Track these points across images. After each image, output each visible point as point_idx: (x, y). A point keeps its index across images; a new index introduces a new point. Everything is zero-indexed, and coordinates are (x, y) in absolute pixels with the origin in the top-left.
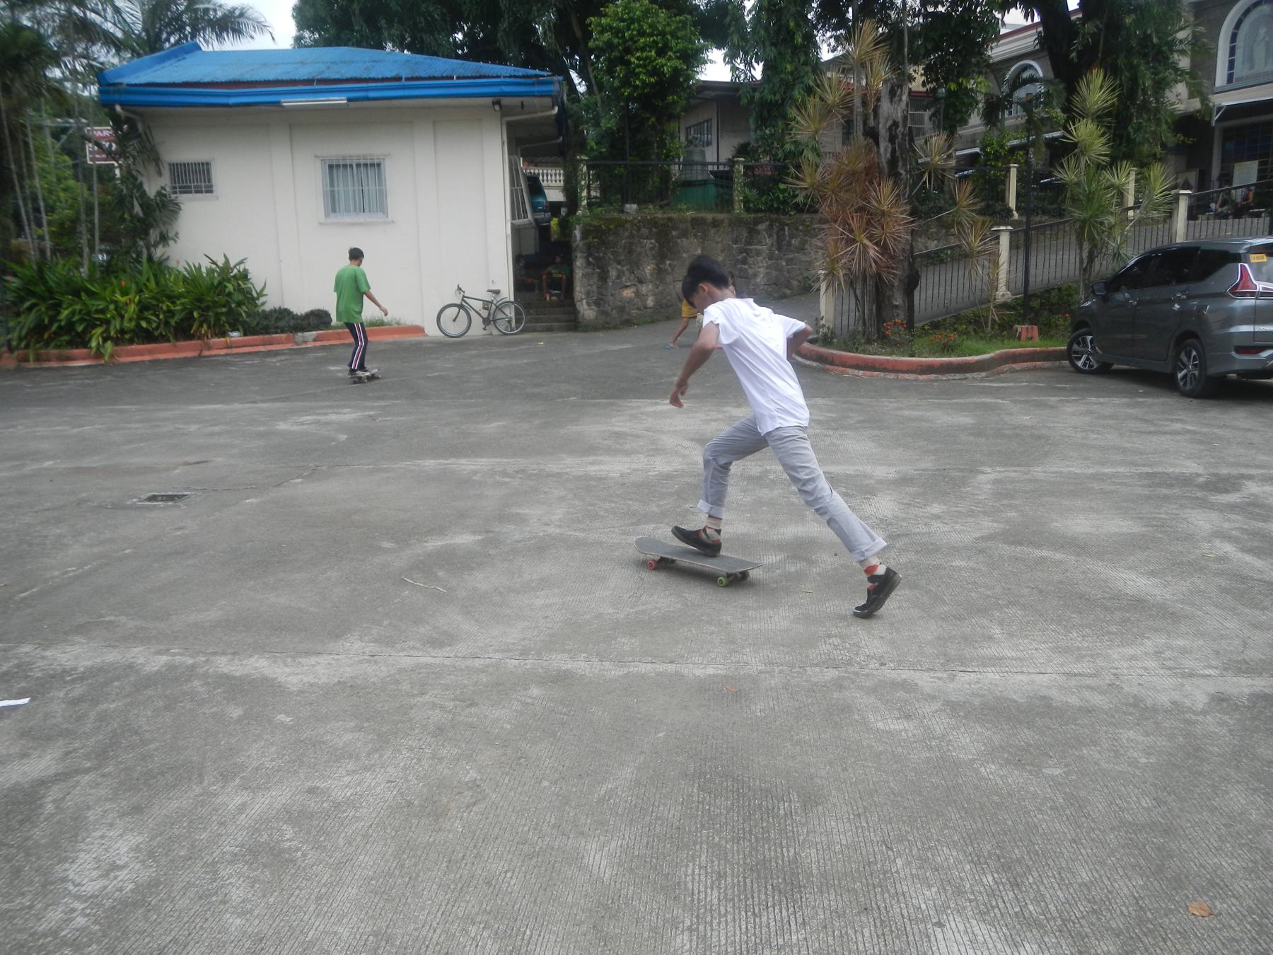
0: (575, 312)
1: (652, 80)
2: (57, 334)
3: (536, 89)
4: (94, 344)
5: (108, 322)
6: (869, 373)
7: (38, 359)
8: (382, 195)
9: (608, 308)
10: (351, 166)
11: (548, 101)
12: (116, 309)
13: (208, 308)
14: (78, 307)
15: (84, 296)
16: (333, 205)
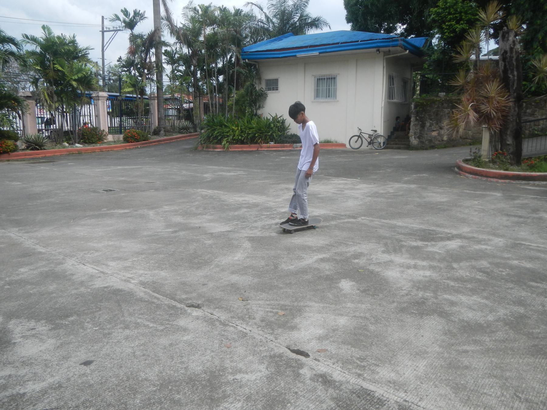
0: (409, 141)
1: (452, 35)
2: (214, 139)
3: (391, 44)
4: (223, 144)
5: (228, 136)
6: (474, 176)
7: (207, 147)
8: (335, 90)
9: (424, 140)
10: (324, 79)
11: (399, 49)
12: (232, 132)
13: (262, 133)
14: (220, 130)
15: (223, 126)
16: (317, 95)
